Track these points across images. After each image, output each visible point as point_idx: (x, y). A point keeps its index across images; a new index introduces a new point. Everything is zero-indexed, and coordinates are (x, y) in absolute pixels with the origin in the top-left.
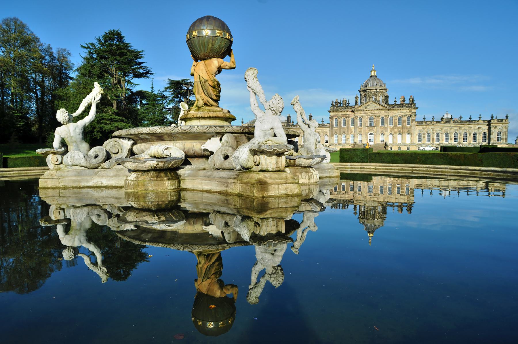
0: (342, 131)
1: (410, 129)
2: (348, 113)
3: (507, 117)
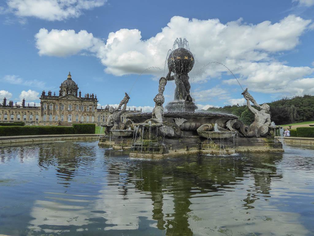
0: (50, 112)
1: (94, 114)
2: (54, 101)
3: (141, 110)
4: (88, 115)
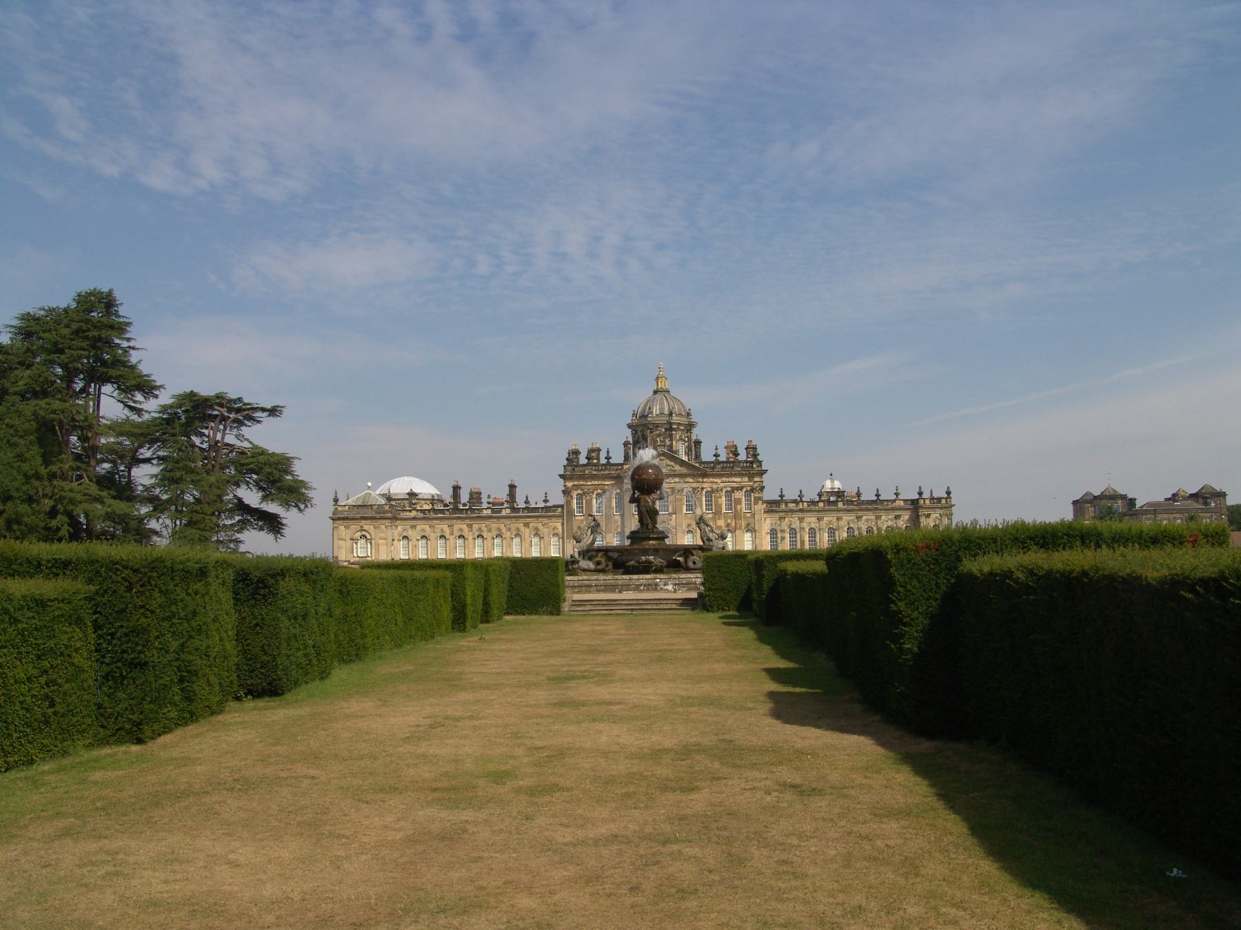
1: (751, 520)
3: (948, 493)
4: (728, 525)
